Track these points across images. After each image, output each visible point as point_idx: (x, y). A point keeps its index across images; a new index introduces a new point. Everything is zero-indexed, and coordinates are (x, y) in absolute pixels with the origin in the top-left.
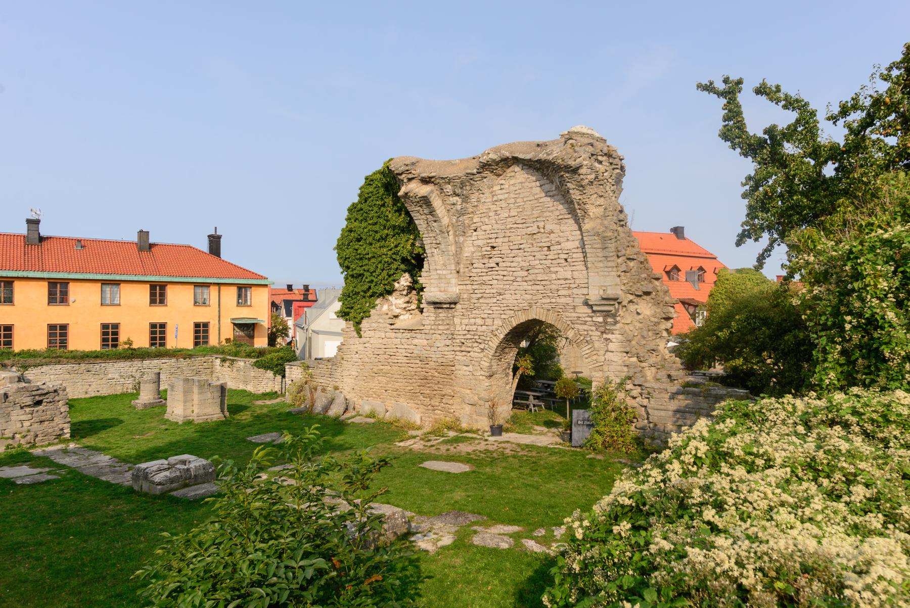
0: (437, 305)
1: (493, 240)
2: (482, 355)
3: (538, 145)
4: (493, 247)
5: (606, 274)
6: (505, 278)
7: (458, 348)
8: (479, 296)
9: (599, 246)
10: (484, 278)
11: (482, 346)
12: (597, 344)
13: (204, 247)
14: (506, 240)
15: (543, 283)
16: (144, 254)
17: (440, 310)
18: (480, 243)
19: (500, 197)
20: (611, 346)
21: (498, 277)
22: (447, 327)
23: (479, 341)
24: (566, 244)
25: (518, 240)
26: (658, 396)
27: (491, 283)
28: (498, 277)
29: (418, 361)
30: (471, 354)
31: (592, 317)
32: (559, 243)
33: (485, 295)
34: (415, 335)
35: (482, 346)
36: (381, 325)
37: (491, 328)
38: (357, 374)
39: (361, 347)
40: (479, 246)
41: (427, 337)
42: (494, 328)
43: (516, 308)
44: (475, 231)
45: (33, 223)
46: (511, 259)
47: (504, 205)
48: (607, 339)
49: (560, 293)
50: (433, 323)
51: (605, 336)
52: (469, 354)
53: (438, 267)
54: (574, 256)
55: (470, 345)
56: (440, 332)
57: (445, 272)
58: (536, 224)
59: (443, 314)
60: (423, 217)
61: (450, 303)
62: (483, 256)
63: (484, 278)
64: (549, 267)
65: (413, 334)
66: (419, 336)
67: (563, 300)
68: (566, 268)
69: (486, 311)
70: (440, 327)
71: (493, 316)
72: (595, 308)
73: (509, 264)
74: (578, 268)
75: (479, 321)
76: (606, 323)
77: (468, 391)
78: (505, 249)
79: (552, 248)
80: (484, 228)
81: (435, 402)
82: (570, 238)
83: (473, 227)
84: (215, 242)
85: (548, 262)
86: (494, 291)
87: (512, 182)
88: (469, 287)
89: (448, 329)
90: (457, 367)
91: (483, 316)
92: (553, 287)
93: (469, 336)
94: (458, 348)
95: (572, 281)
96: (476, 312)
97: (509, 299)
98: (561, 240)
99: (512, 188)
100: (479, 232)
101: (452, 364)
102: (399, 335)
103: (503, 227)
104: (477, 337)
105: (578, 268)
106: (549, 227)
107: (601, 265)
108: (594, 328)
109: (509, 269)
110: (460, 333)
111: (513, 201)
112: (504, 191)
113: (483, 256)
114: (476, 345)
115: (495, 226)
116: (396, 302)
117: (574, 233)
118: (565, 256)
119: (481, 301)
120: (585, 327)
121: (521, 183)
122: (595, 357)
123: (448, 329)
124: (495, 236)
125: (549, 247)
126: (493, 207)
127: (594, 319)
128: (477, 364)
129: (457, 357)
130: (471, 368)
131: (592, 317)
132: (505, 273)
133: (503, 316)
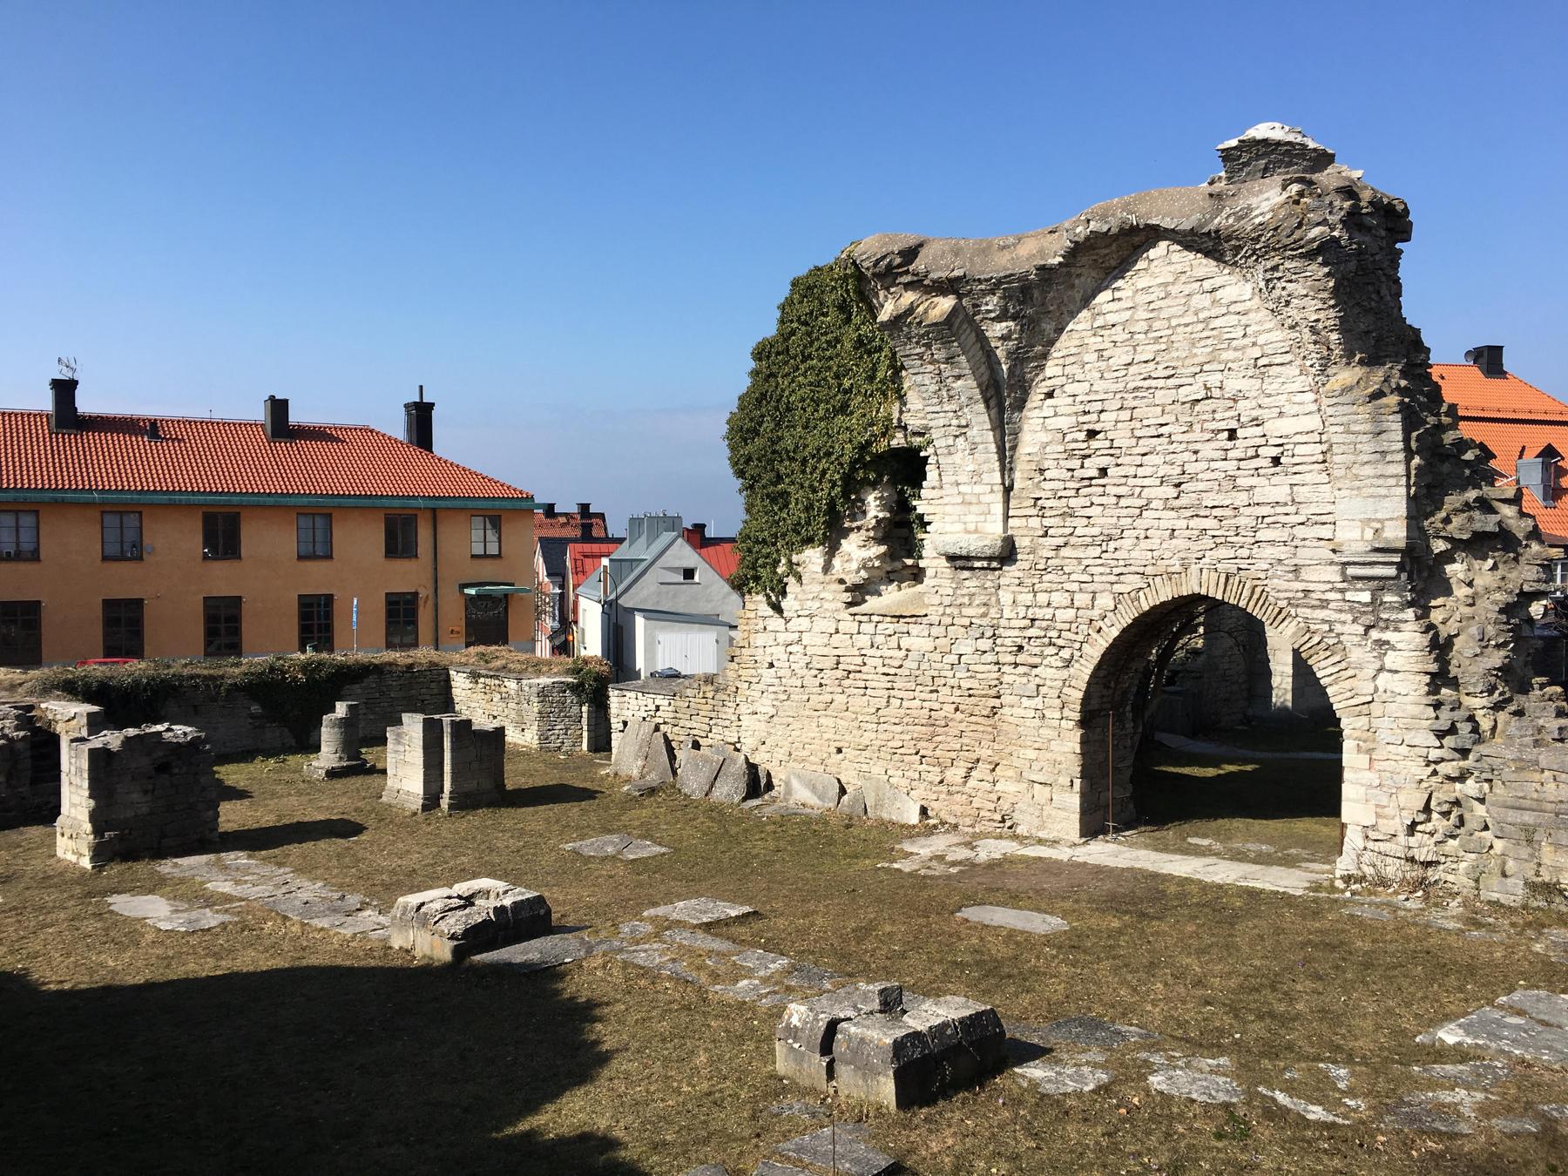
0: (960, 561)
1: (1094, 417)
2: (1065, 674)
4: (1092, 434)
5: (1383, 491)
6: (1123, 502)
7: (1010, 659)
8: (1061, 541)
9: (1367, 427)
10: (1072, 502)
11: (1066, 654)
12: (1356, 655)
13: (397, 427)
14: (1125, 415)
15: (1216, 512)
16: (282, 447)
17: (966, 574)
18: (1064, 423)
19: (1111, 319)
20: (1391, 660)
21: (1104, 500)
22: (983, 609)
23: (1060, 642)
24: (1279, 422)
25: (1153, 415)
26: (1513, 777)
27: (1088, 512)
28: (1104, 500)
29: (912, 685)
31: (1342, 591)
32: (1257, 422)
33: (1073, 540)
35: (1066, 654)
38: (772, 711)
39: (779, 653)
41: (935, 631)
42: (1095, 613)
43: (1149, 570)
44: (1050, 395)
45: (64, 390)
46: (1138, 460)
48: (1381, 643)
49: (1260, 536)
50: (947, 601)
51: (1375, 634)
52: (1035, 671)
53: (961, 479)
54: (1299, 450)
55: (1037, 650)
56: (966, 622)
57: (978, 489)
58: (1200, 379)
59: (971, 583)
60: (930, 368)
61: (990, 559)
62: (1070, 454)
63: (1072, 502)
64: (1234, 478)
65: (901, 626)
67: (1269, 552)
68: (1274, 480)
69: (1073, 577)
70: (966, 611)
73: (1132, 471)
74: (1308, 478)
76: (1375, 603)
77: (1032, 754)
78: (1122, 438)
79: (1240, 433)
80: (1070, 389)
81: (955, 774)
83: (1044, 388)
84: (421, 416)
85: (1231, 466)
89: (984, 615)
90: (1005, 699)
91: (1067, 586)
92: (1241, 521)
93: (1032, 632)
94: (1010, 659)
95: (1292, 509)
97: (1131, 551)
99: (1142, 298)
100: (1059, 400)
101: (993, 692)
102: (868, 628)
103: (1120, 386)
104: (1054, 634)
105: (1308, 478)
106: (1233, 384)
107: (1368, 470)
108: (1349, 617)
109: (1131, 481)
110: (1015, 623)
111: (1143, 326)
112: (1123, 304)
113: (1070, 454)
114: (1052, 650)
115: (1100, 386)
116: (858, 551)
117: (1299, 398)
118: (1275, 452)
119: (1065, 552)
121: (1166, 284)
122: (1348, 684)
123: (984, 615)
124: (1098, 406)
126: (1094, 342)
127: (1349, 596)
131: (1342, 591)
132: (1122, 490)
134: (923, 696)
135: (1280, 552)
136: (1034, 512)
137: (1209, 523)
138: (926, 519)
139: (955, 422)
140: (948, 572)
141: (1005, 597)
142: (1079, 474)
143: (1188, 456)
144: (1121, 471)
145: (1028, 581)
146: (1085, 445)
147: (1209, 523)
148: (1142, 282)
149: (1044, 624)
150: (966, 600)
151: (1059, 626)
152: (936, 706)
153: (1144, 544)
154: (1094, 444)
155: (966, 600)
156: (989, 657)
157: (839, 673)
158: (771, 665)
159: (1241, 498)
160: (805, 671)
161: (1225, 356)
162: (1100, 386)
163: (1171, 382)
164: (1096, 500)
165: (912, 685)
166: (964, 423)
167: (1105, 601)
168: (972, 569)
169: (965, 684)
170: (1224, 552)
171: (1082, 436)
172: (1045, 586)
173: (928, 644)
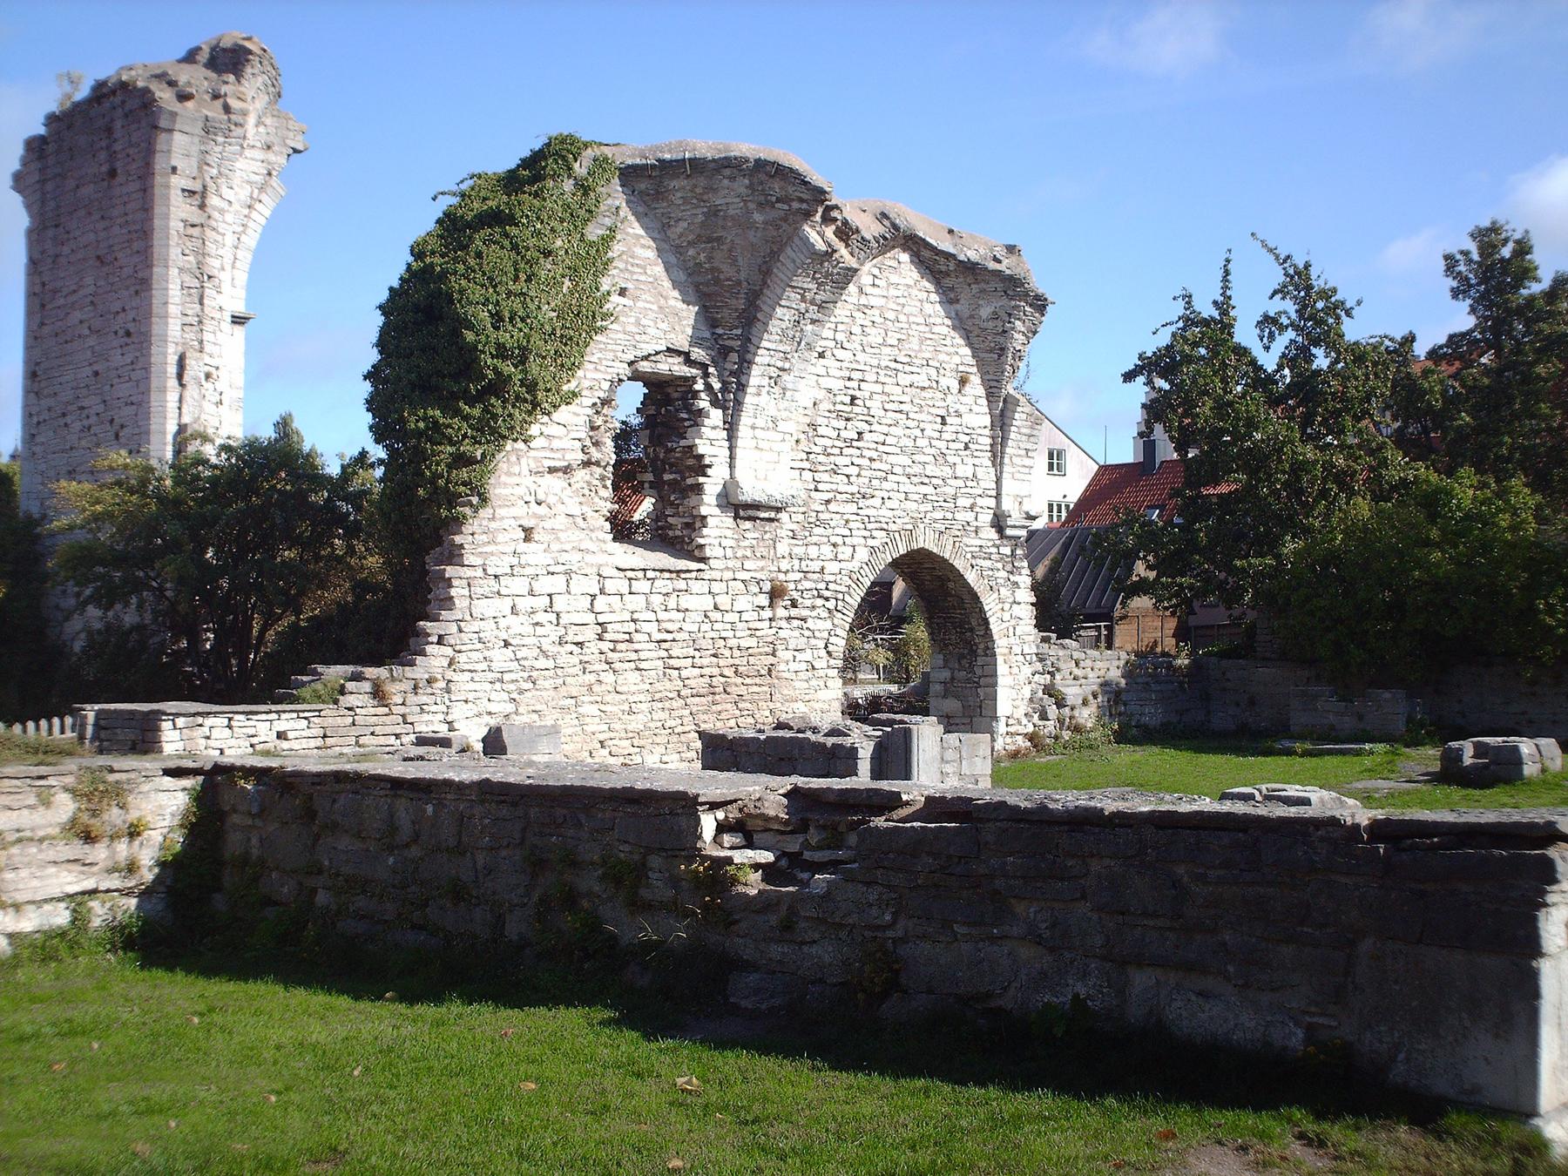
2: (828, 624)
3: (951, 232)
6: (875, 465)
8: (830, 495)
10: (841, 461)
11: (831, 604)
14: (878, 388)
15: (934, 481)
17: (748, 525)
18: (837, 385)
19: (873, 301)
23: (827, 594)
29: (691, 652)
30: (810, 623)
34: (681, 585)
35: (831, 604)
36: (589, 558)
37: (849, 566)
38: (510, 708)
40: (829, 391)
41: (716, 587)
42: (855, 565)
43: (892, 527)
44: (821, 355)
47: (878, 320)
53: (760, 423)
54: (981, 440)
55: (808, 603)
63: (841, 461)
66: (696, 586)
69: (837, 531)
71: (855, 541)
72: (1009, 532)
73: (881, 438)
75: (827, 550)
78: (875, 405)
79: (949, 420)
80: (840, 353)
82: (975, 408)
86: (854, 489)
87: (894, 278)
88: (808, 475)
91: (833, 539)
93: (808, 585)
96: (817, 531)
98: (962, 409)
101: (769, 650)
102: (642, 586)
103: (875, 362)
109: (881, 448)
114: (820, 602)
115: (861, 357)
118: (967, 439)
120: (987, 563)
125: (943, 418)
128: (821, 644)
129: (782, 634)
130: (807, 655)
132: (874, 455)
133: (871, 542)
134: (705, 661)
135: (970, 516)
136: (806, 465)
137: (929, 490)
138: (707, 461)
139: (780, 364)
140: (729, 521)
141: (782, 548)
142: (844, 434)
143: (918, 432)
144: (874, 437)
145: (800, 534)
146: (848, 409)
147: (929, 490)
148: (894, 278)
149: (816, 576)
150: (749, 553)
151: (828, 578)
152: (716, 671)
153: (889, 504)
154: (856, 410)
155: (749, 553)
156: (767, 614)
157: (605, 646)
158: (507, 644)
159: (947, 471)
160: (557, 648)
161: (942, 357)
162: (861, 357)
163: (908, 369)
164: (856, 461)
165: (691, 652)
166: (787, 366)
167: (863, 554)
168: (753, 519)
169: (744, 643)
170: (939, 515)
171: (847, 400)
172: (814, 539)
173: (707, 602)
